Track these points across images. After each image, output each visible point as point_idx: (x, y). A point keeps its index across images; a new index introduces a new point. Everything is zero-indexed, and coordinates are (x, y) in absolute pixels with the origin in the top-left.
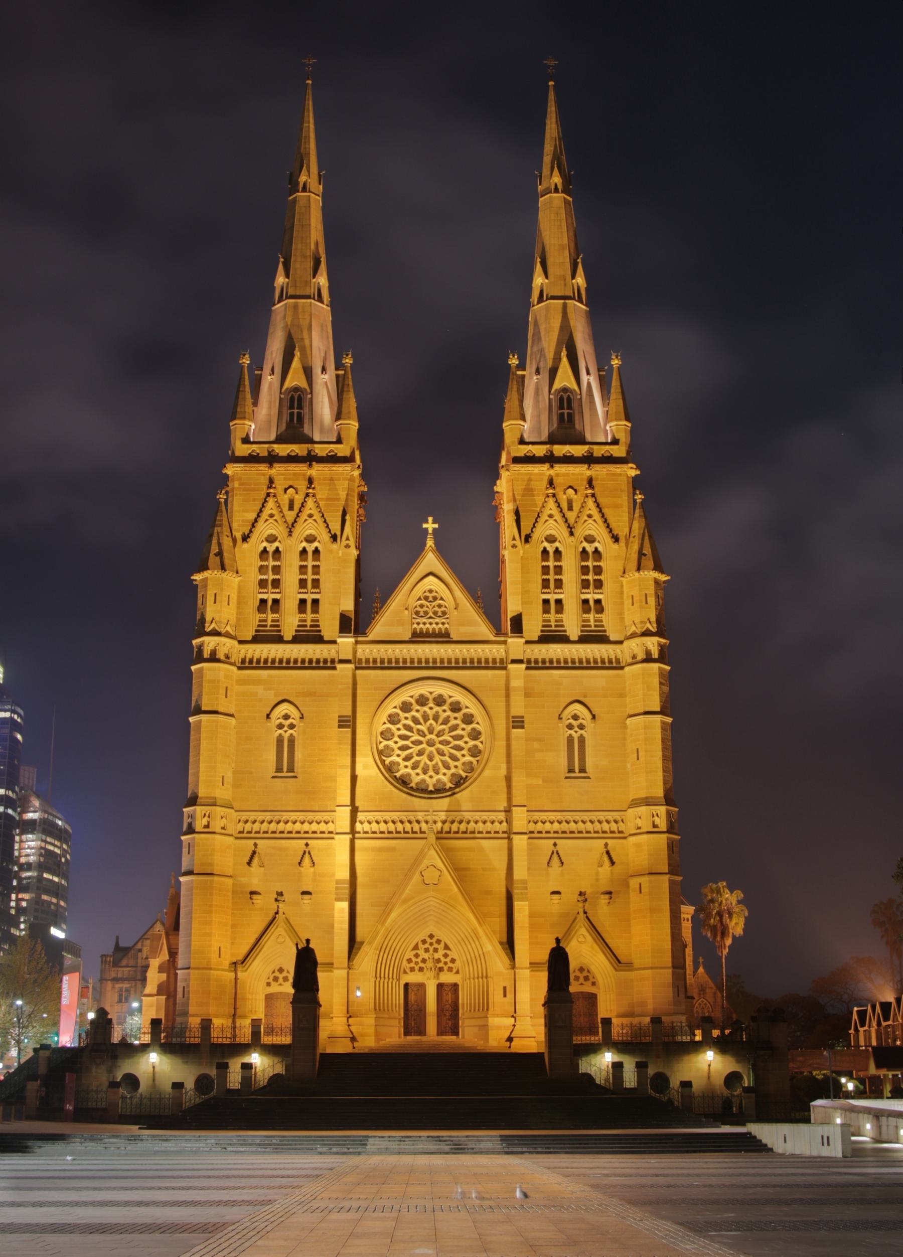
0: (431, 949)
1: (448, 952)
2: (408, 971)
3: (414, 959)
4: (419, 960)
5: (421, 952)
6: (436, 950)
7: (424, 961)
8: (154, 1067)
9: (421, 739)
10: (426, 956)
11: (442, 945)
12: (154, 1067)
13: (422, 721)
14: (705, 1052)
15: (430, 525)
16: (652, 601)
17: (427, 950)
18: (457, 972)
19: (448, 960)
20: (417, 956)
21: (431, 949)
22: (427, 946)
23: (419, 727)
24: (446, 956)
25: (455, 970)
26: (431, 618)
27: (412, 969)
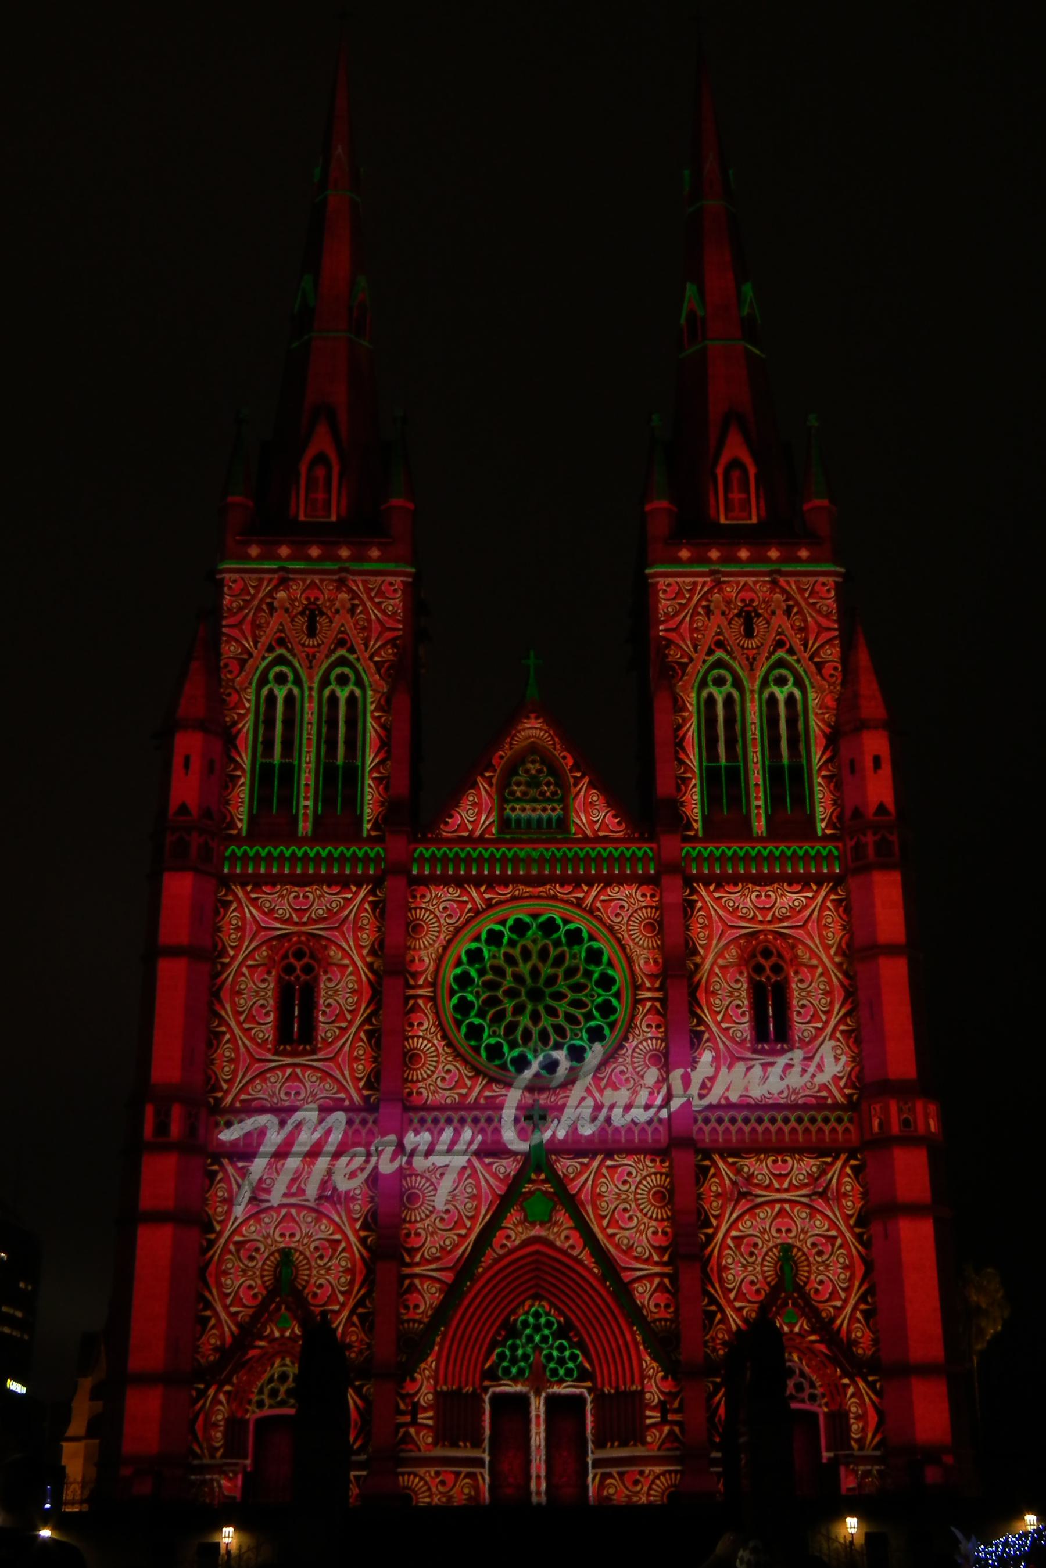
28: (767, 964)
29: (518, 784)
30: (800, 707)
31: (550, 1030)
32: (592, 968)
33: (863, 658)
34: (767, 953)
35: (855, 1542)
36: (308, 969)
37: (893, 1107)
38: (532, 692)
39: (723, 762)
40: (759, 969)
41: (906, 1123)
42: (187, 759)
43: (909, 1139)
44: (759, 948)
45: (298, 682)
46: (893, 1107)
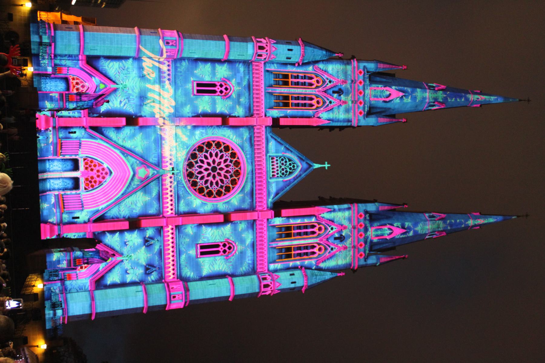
0: (99, 174)
1: (97, 183)
2: (86, 161)
3: (93, 164)
4: (93, 167)
5: (97, 168)
6: (98, 176)
7: (92, 170)
8: (22, 5)
9: (216, 164)
10: (95, 171)
11: (102, 180)
12: (22, 5)
13: (226, 164)
14: (46, 343)
15: (326, 166)
16: (293, 286)
17: (98, 171)
18: (85, 189)
19: (93, 183)
20: (95, 166)
21: (99, 174)
22: (101, 171)
23: (223, 162)
24: (95, 182)
25: (87, 187)
26: (281, 167)
27: (86, 164)
28: (226, 248)
29: (286, 162)
30: (311, 256)
31: (202, 175)
32: (224, 188)
33: (328, 276)
34: (230, 248)
35: (34, 288)
36: (221, 92)
37: (180, 292)
38: (317, 166)
39: (293, 232)
40: (224, 245)
41: (174, 297)
42: (291, 50)
43: (171, 298)
44: (231, 246)
45: (317, 87)
46: (180, 292)
